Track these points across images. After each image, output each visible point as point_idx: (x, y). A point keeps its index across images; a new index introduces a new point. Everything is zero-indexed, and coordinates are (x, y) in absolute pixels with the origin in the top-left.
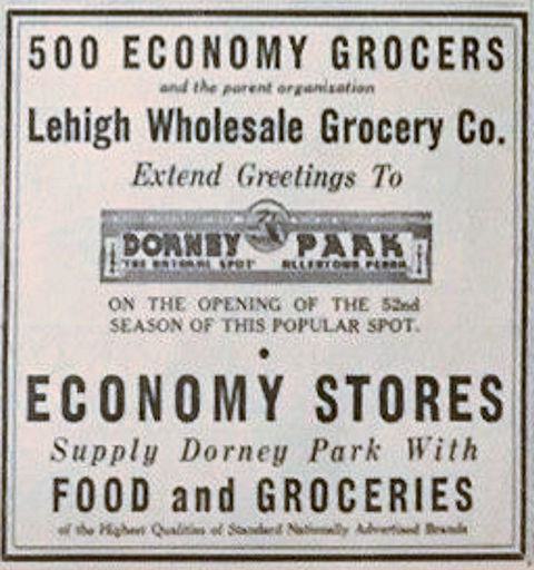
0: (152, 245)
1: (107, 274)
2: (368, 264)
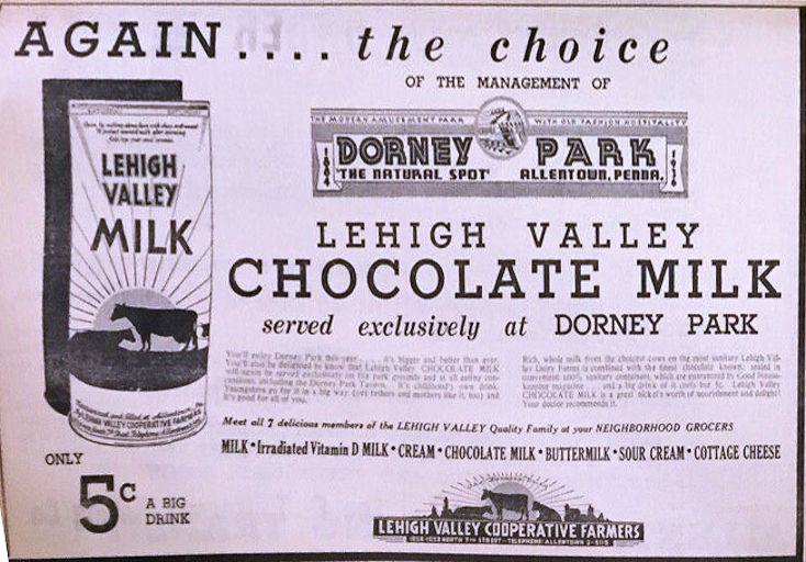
0: (371, 151)
1: (322, 186)
2: (617, 174)
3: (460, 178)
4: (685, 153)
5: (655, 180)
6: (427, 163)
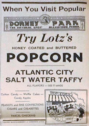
0: (17, 24)
2: (70, 27)
3: (36, 28)
4: (85, 23)
5: (78, 28)
6: (29, 26)
